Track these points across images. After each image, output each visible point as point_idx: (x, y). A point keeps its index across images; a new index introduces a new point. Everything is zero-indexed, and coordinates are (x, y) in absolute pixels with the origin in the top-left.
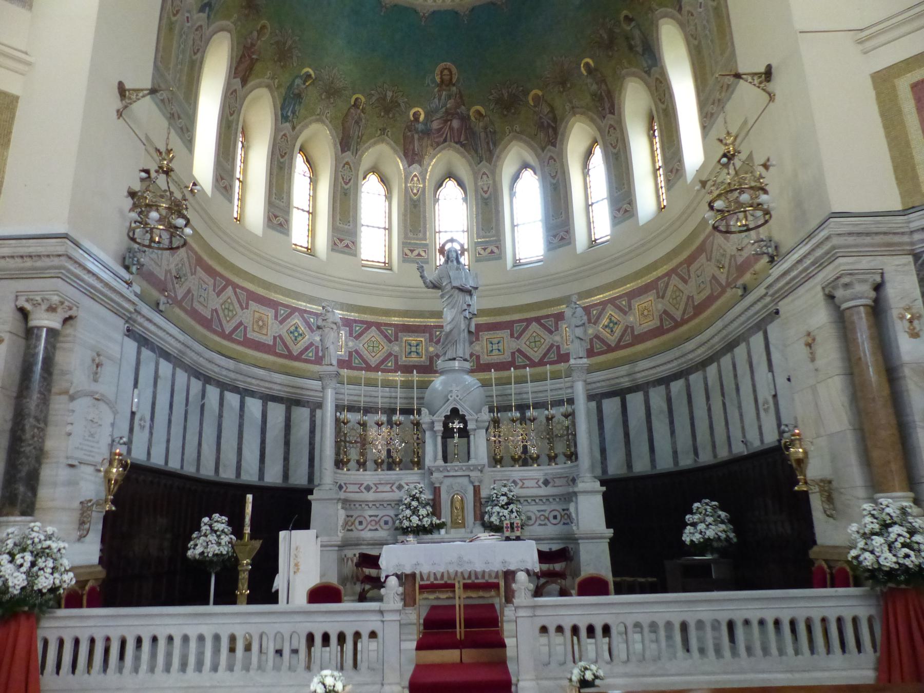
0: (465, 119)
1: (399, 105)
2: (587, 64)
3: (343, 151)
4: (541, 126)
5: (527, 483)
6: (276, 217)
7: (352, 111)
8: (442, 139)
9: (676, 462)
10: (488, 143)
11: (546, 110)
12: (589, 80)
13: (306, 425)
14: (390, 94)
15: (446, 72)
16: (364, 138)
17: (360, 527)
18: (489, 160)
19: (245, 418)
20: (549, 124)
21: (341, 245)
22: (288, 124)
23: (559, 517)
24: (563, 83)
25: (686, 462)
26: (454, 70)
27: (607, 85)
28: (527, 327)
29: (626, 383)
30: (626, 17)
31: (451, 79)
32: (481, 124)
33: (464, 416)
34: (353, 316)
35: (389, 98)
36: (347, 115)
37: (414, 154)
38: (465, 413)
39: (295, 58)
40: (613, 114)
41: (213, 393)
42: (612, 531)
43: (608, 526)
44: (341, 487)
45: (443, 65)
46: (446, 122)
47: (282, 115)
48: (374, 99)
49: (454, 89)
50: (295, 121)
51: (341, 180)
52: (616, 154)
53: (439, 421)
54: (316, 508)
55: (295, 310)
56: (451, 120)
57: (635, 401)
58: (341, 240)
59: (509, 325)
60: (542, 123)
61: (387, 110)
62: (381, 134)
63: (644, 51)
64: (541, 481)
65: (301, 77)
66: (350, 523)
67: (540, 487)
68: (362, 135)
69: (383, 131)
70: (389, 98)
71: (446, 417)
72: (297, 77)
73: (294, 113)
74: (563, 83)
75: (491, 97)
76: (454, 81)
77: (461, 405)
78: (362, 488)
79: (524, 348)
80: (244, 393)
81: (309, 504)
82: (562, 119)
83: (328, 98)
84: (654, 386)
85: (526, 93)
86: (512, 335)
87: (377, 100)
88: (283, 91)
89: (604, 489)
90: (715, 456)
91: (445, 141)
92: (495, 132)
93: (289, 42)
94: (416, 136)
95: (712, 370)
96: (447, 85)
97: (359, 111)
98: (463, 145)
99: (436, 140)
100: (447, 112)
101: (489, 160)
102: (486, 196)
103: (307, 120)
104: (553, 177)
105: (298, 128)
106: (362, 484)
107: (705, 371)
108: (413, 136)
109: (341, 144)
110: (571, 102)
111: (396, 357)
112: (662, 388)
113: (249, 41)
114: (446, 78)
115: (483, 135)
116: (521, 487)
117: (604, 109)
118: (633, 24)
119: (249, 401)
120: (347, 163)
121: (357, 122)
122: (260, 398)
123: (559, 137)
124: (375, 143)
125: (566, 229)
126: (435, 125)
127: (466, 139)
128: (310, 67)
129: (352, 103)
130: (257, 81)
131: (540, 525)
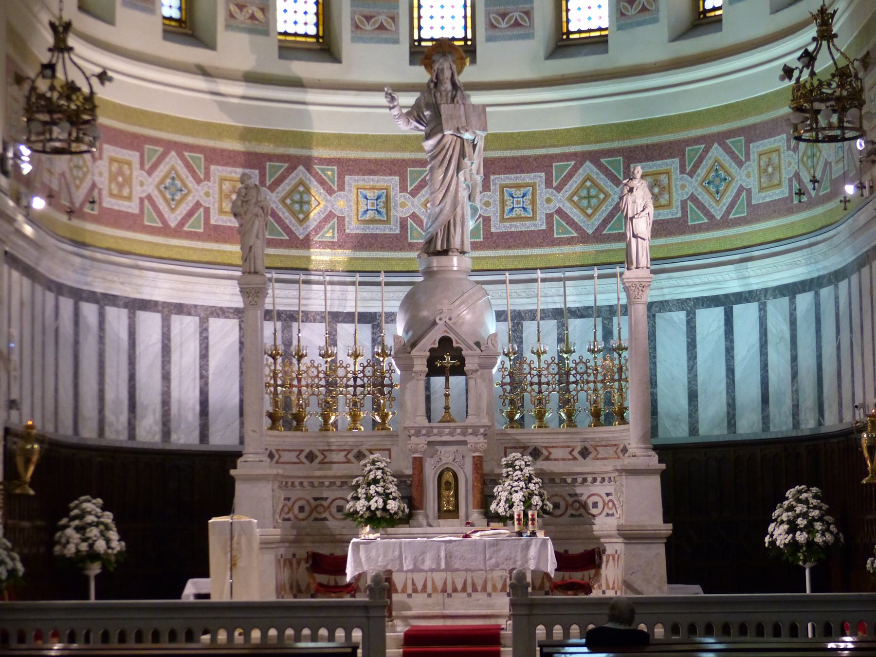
5: (556, 453)
9: (796, 424)
13: (193, 348)
17: (301, 516)
19: (107, 341)
21: (241, 17)
23: (600, 505)
25: (809, 424)
28: (575, 169)
29: (734, 287)
33: (460, 350)
34: (266, 148)
38: (462, 346)
41: (67, 304)
42: (670, 526)
43: (665, 522)
44: (271, 456)
53: (421, 357)
54: (240, 489)
55: (169, 146)
57: (746, 316)
58: (241, 7)
59: (543, 164)
64: (578, 449)
66: (286, 509)
67: (575, 459)
71: (431, 350)
77: (456, 334)
78: (302, 457)
79: (569, 208)
80: (104, 300)
81: (232, 481)
84: (775, 297)
86: (548, 183)
89: (663, 466)
90: (841, 420)
95: (843, 285)
106: (301, 451)
107: (837, 287)
111: (341, 220)
112: (786, 300)
116: (547, 459)
119: (111, 312)
122: (126, 306)
131: (572, 516)
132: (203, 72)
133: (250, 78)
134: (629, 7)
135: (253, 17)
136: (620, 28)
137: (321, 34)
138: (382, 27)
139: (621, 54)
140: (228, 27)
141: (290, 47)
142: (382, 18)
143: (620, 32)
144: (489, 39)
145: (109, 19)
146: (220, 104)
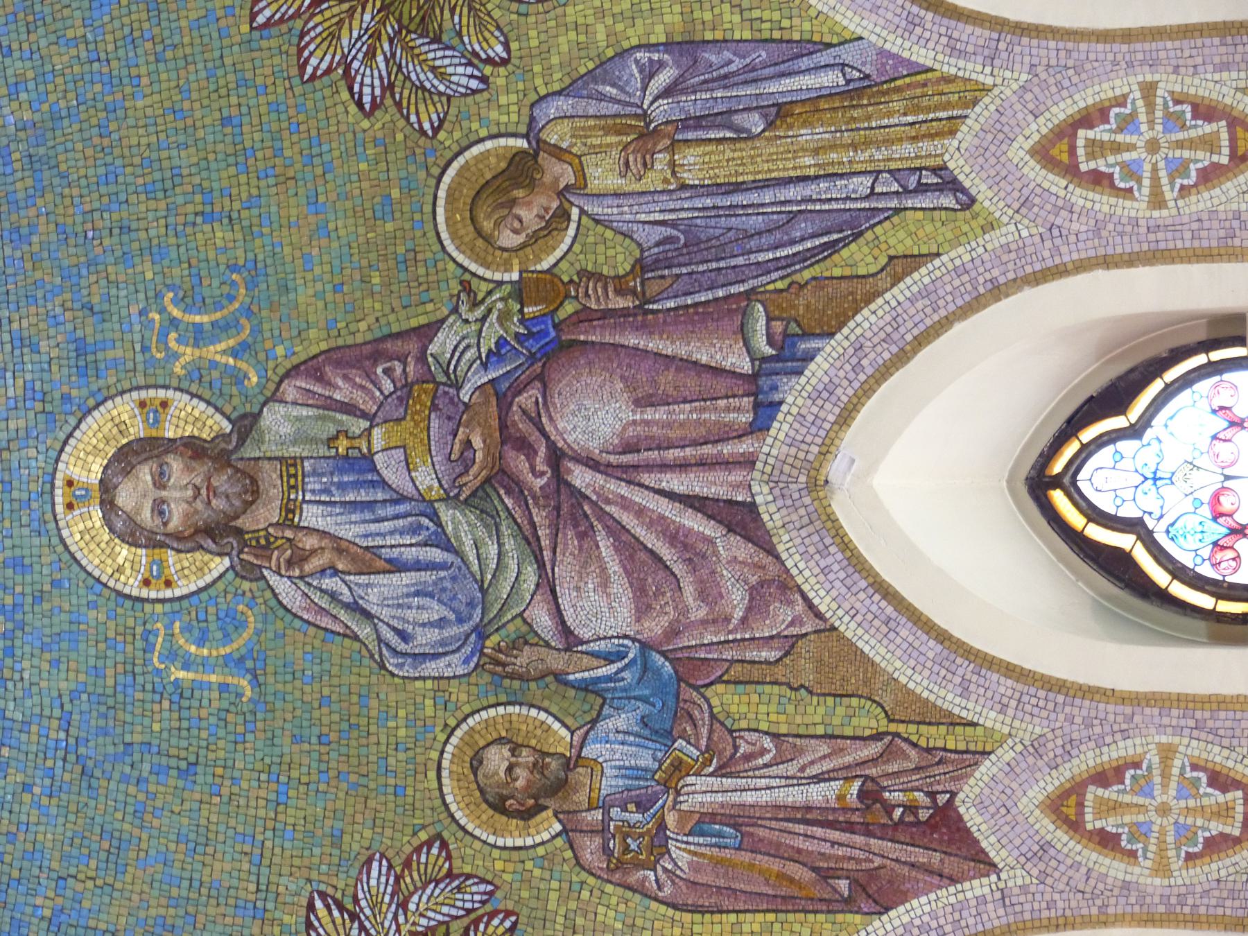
8: (731, 548)
15: (134, 494)
26: (121, 417)
31: (194, 449)
32: (603, 175)
45: (84, 529)
46: (572, 510)
49: (278, 423)
56: (557, 457)
75: (369, 83)
76: (191, 417)
91: (740, 518)
92: (685, 47)
94: (703, 791)
96: (253, 492)
98: (788, 356)
99: (736, 599)
100: (487, 491)
108: (702, 823)
114: (183, 492)
115: (695, 163)
127: (728, 314)
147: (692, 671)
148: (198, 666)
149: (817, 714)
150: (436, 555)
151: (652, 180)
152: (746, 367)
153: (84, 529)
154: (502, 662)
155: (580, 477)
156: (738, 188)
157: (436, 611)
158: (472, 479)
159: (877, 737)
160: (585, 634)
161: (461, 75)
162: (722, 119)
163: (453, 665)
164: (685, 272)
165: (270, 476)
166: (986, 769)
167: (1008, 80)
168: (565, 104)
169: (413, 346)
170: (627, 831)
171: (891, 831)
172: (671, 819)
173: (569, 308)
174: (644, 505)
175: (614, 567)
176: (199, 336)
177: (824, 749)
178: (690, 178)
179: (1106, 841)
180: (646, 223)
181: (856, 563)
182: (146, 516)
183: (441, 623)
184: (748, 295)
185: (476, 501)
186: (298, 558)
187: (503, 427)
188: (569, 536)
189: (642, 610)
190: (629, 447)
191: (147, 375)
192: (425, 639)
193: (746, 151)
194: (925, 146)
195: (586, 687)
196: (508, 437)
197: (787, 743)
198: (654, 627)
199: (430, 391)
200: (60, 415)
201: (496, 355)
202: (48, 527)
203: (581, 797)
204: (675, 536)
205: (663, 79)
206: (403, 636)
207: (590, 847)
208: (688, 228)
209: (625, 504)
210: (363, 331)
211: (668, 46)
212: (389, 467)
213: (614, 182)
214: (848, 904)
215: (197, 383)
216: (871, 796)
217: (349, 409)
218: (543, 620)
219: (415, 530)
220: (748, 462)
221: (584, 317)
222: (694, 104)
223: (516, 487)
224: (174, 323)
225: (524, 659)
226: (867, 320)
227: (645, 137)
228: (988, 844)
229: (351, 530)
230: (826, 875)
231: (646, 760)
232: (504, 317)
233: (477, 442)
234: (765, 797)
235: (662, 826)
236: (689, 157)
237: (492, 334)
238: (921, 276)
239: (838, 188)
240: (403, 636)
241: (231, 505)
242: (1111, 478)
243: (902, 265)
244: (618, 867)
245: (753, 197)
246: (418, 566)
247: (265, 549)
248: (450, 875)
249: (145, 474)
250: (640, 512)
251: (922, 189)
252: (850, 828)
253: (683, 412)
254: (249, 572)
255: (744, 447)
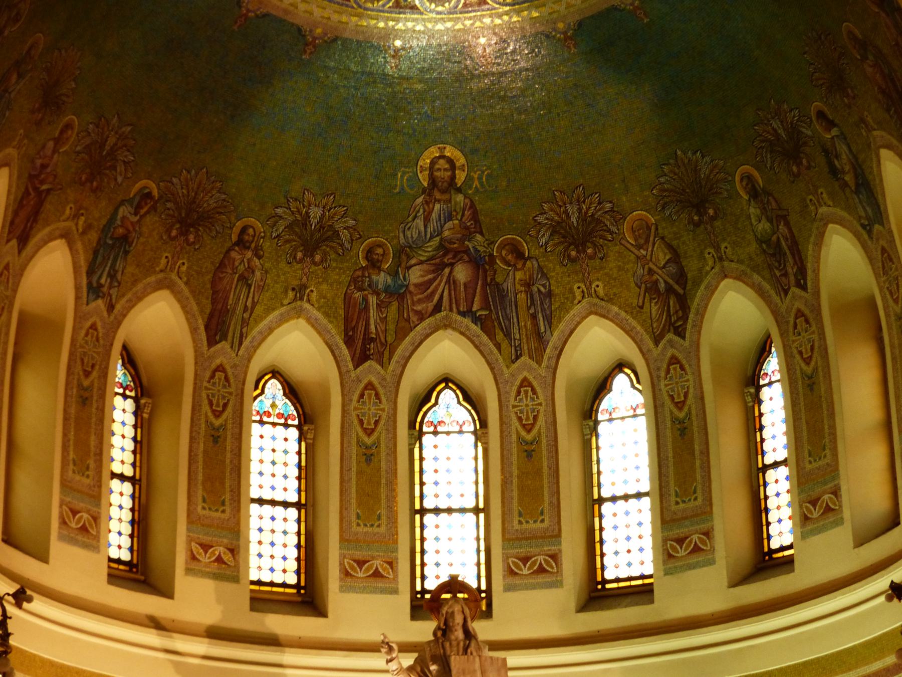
0: (481, 265)
1: (336, 233)
2: (748, 179)
3: (211, 342)
4: (652, 289)
6: (74, 512)
7: (233, 254)
8: (431, 306)
10: (534, 317)
11: (662, 256)
12: (753, 211)
14: (315, 213)
16: (259, 309)
18: (537, 355)
20: (670, 290)
21: (205, 558)
22: (100, 302)
24: (699, 206)
26: (461, 160)
27: (787, 224)
30: (821, 115)
31: (453, 177)
32: (519, 275)
35: (314, 222)
36: (222, 265)
37: (368, 339)
39: (121, 168)
40: (804, 288)
45: (434, 152)
46: (439, 268)
47: (89, 284)
48: (281, 226)
49: (460, 198)
50: (114, 292)
51: (206, 408)
52: (810, 378)
56: (452, 265)
58: (206, 547)
60: (657, 281)
61: (309, 252)
62: (295, 300)
63: (857, 185)
65: (130, 201)
68: (254, 304)
69: (300, 291)
70: (314, 222)
72: (122, 203)
73: (112, 276)
74: (699, 206)
75: (541, 219)
76: (461, 177)
82: (697, 283)
83: (184, 233)
85: (619, 216)
87: (290, 227)
88: (93, 236)
91: (438, 309)
92: (550, 294)
93: (112, 141)
94: (373, 300)
96: (443, 192)
97: (249, 254)
98: (476, 320)
99: (418, 308)
100: (444, 247)
101: (537, 355)
102: (529, 437)
103: (140, 286)
104: (680, 405)
105: (118, 307)
108: (365, 299)
109: (207, 327)
110: (717, 248)
113: (39, 162)
115: (522, 297)
117: (785, 275)
118: (835, 132)
120: (220, 368)
121: (243, 278)
123: (691, 316)
124: (282, 320)
125: (704, 527)
126: (416, 276)
127: (486, 305)
128: (149, 178)
129: (234, 238)
130: (47, 230)
132: (156, 624)
133: (215, 634)
134: (678, 547)
135: (219, 560)
136: (667, 573)
137: (303, 584)
138: (377, 574)
139: (669, 605)
140: (189, 571)
141: (264, 599)
142: (377, 563)
143: (667, 577)
144: (508, 588)
145: (42, 556)
146: (176, 665)
147: (401, 297)
148: (401, 179)
149: (391, 327)
150: (428, 236)
151: (518, 287)
152: (474, 309)
153: (434, 151)
154: (404, 253)
155: (447, 270)
156: (516, 307)
157: (415, 236)
158: (447, 244)
159: (386, 341)
160: (410, 272)
161: (543, 241)
162: (533, 303)
163: (402, 240)
164: (496, 296)
165: (446, 197)
166: (379, 367)
167: (542, 371)
168: (536, 265)
169: (478, 230)
170: (363, 282)
171: (364, 344)
172: (366, 292)
173: (487, 267)
174: (441, 287)
175: (426, 278)
176: (480, 178)
177: (383, 329)
178: (518, 296)
179: (362, 396)
180: (508, 285)
181: (427, 336)
182: (437, 166)
183: (412, 237)
184: (491, 310)
185: (441, 246)
186: (427, 203)
187: (459, 252)
188: (433, 268)
189: (416, 285)
190: (454, 282)
191: (471, 166)
192: (408, 234)
193: (525, 309)
194: (526, 351)
195: (397, 273)
196: (456, 253)
197: (384, 320)
198: (412, 288)
199: (467, 233)
200: (460, 146)
201: (476, 250)
202: (435, 143)
203: (371, 271)
204: (433, 293)
205: (542, 289)
206: (409, 228)
207: (359, 273)
208: (507, 295)
209: (441, 281)
210: (482, 218)
211: (550, 290)
212: (449, 224)
213: (518, 278)
214: (346, 335)
215: (469, 179)
216: (372, 340)
217: (463, 215)
218: (413, 261)
219: (434, 231)
220: (451, 310)
221: (485, 271)
222: (537, 297)
223: (445, 255)
224: (483, 172)
225: (404, 257)
226: (485, 338)
227: (528, 285)
228: (361, 368)
229: (434, 215)
230: (353, 329)
231: (380, 286)
232: (485, 252)
233: (455, 246)
234: (371, 315)
235: (364, 290)
236: (523, 295)
237: (481, 249)
238: (495, 351)
239: (516, 331)
240: (409, 228)
241: (441, 186)
242: (448, 397)
243: (498, 346)
244: (354, 280)
245: (514, 311)
246: (426, 232)
247: (430, 195)
248: (352, 240)
249: (447, 166)
250: (439, 285)
251: (516, 351)
252: (364, 335)
253: (463, 295)
254: (424, 192)
255: (455, 309)
